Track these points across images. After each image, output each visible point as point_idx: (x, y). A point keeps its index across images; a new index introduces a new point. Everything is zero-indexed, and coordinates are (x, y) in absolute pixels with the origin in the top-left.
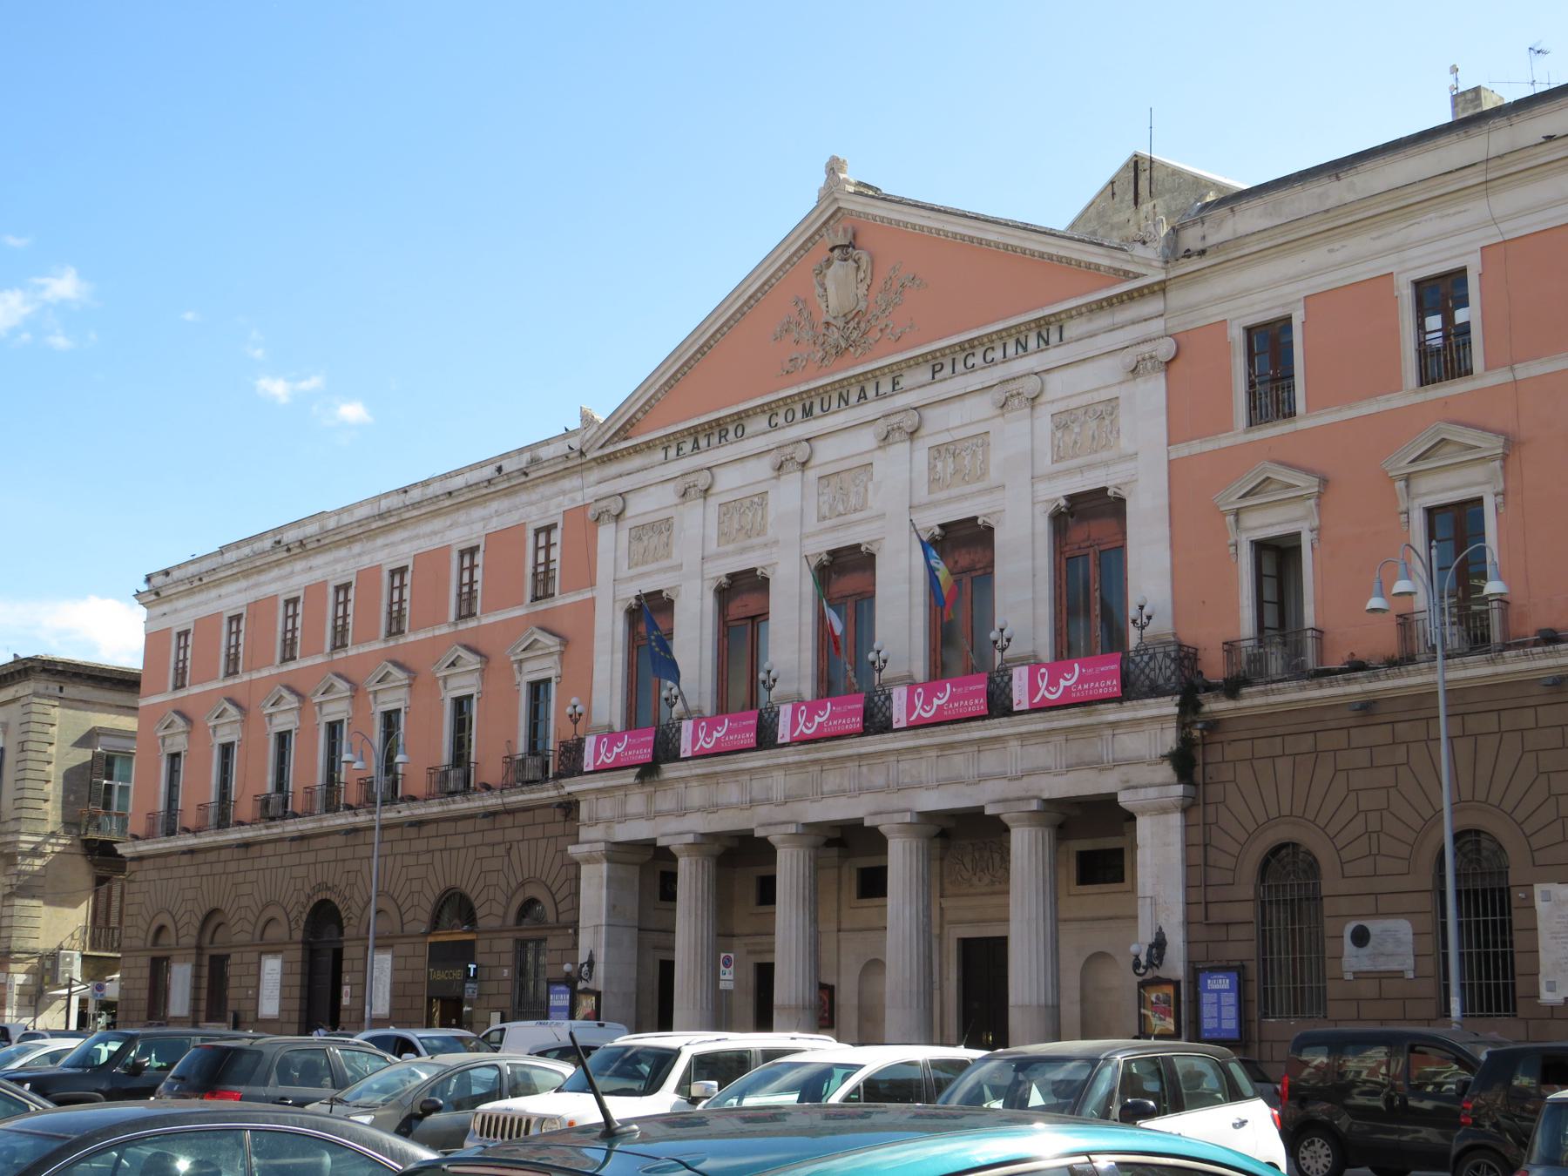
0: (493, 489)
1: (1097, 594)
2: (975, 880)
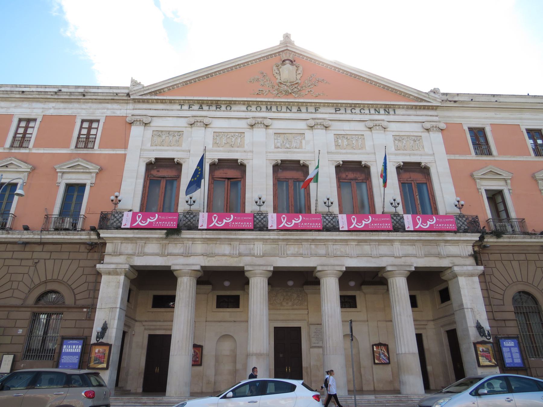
0: (56, 97)
1: (418, 197)
2: (284, 304)
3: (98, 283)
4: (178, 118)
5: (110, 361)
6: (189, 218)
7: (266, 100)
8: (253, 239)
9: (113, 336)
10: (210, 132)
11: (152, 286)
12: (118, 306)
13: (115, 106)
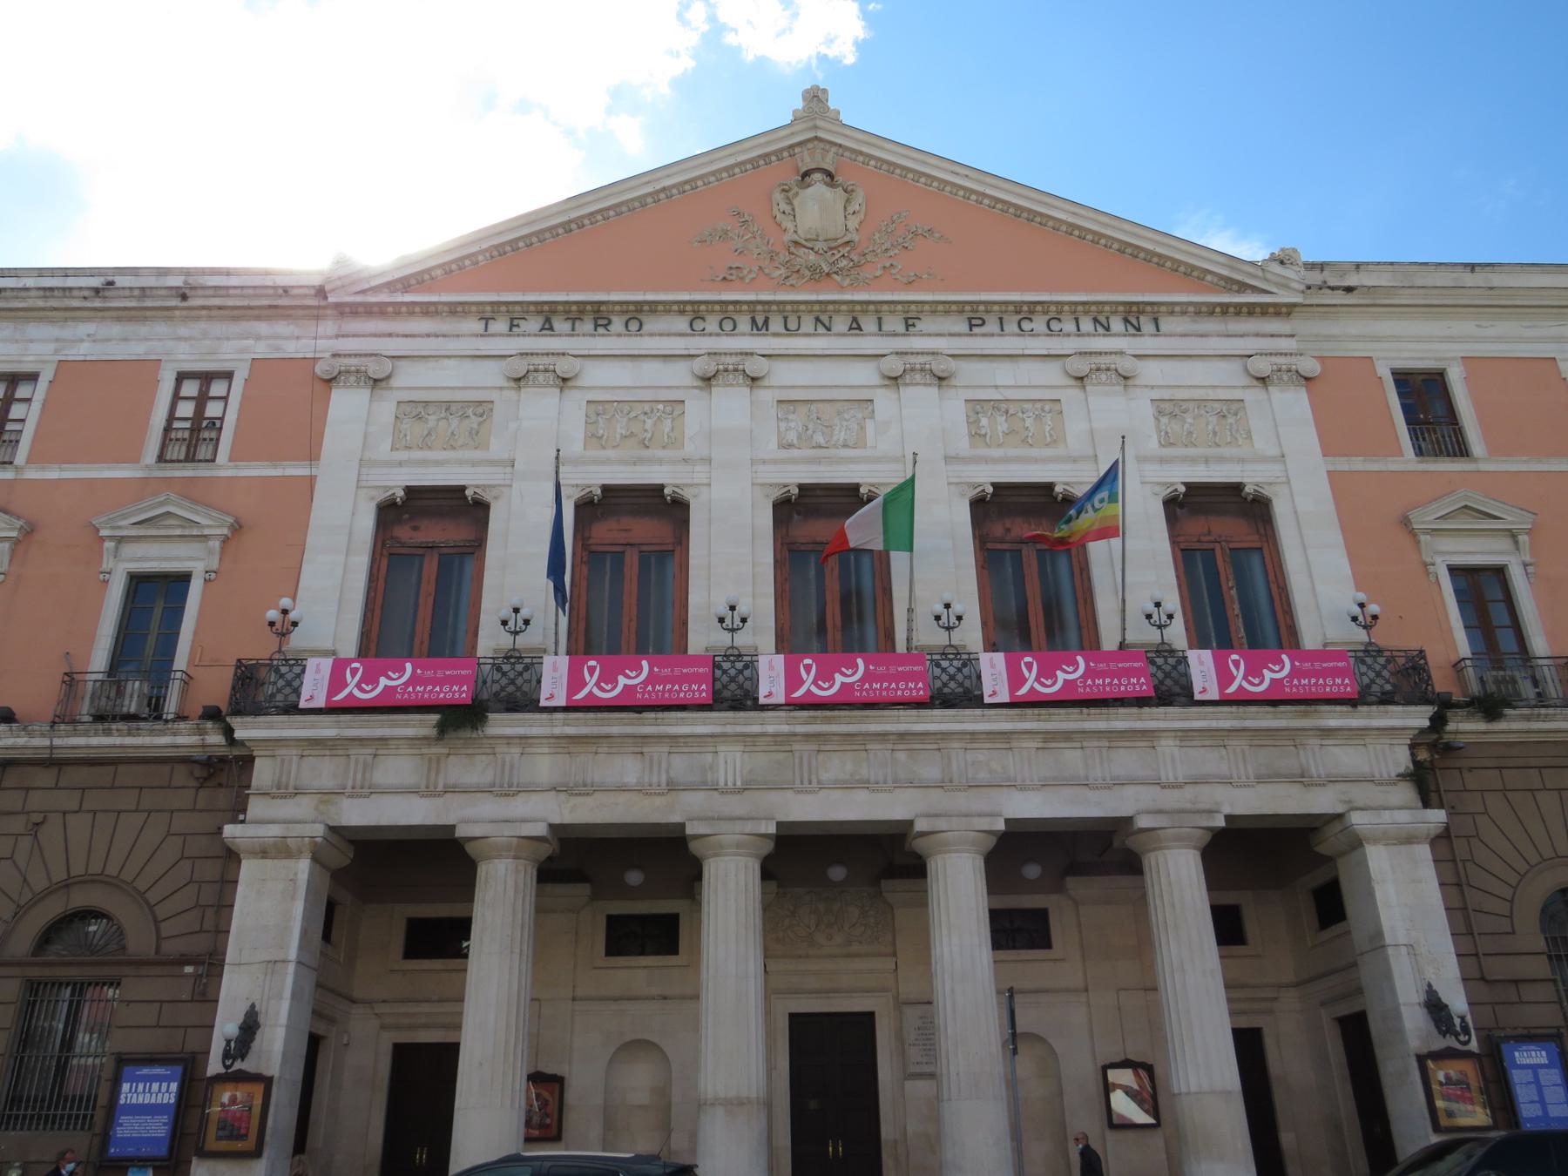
0: (97, 304)
1: (1234, 592)
3: (227, 883)
4: (479, 362)
5: (268, 1131)
6: (512, 675)
7: (751, 297)
8: (712, 736)
9: (275, 1051)
10: (575, 404)
11: (399, 890)
12: (293, 954)
13: (281, 328)
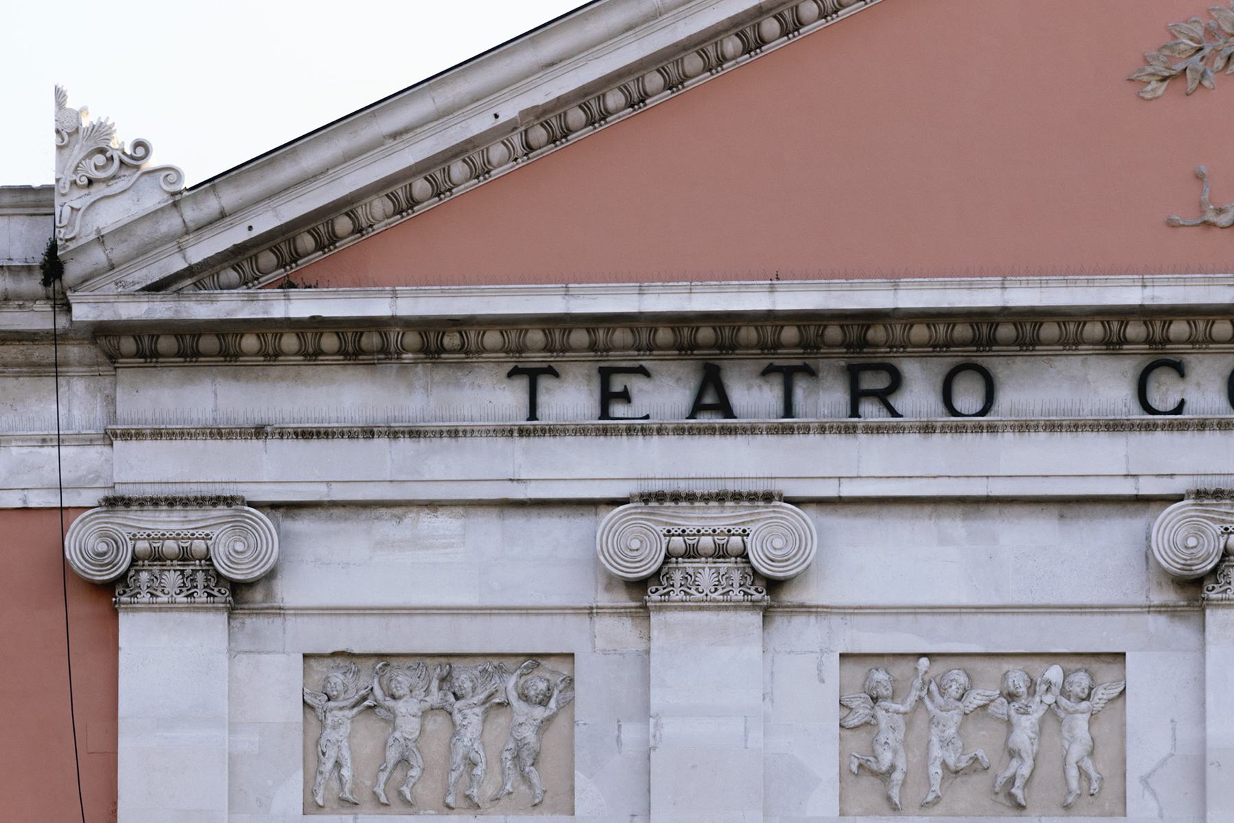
4: (518, 522)
10: (808, 648)
